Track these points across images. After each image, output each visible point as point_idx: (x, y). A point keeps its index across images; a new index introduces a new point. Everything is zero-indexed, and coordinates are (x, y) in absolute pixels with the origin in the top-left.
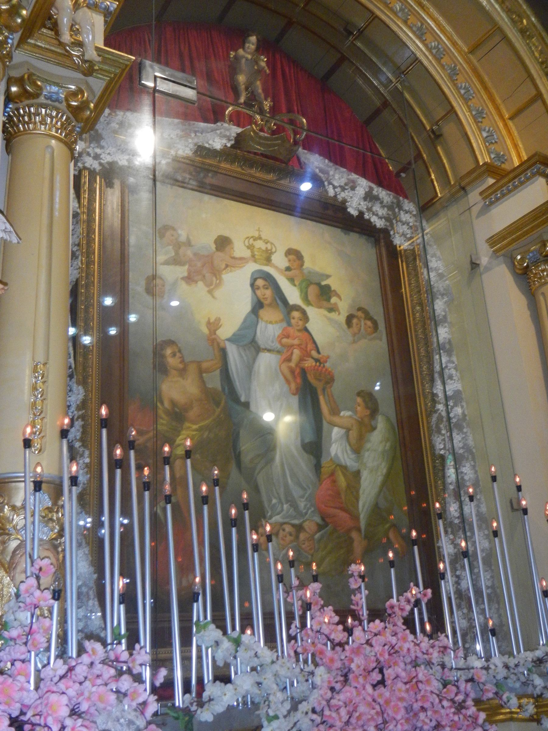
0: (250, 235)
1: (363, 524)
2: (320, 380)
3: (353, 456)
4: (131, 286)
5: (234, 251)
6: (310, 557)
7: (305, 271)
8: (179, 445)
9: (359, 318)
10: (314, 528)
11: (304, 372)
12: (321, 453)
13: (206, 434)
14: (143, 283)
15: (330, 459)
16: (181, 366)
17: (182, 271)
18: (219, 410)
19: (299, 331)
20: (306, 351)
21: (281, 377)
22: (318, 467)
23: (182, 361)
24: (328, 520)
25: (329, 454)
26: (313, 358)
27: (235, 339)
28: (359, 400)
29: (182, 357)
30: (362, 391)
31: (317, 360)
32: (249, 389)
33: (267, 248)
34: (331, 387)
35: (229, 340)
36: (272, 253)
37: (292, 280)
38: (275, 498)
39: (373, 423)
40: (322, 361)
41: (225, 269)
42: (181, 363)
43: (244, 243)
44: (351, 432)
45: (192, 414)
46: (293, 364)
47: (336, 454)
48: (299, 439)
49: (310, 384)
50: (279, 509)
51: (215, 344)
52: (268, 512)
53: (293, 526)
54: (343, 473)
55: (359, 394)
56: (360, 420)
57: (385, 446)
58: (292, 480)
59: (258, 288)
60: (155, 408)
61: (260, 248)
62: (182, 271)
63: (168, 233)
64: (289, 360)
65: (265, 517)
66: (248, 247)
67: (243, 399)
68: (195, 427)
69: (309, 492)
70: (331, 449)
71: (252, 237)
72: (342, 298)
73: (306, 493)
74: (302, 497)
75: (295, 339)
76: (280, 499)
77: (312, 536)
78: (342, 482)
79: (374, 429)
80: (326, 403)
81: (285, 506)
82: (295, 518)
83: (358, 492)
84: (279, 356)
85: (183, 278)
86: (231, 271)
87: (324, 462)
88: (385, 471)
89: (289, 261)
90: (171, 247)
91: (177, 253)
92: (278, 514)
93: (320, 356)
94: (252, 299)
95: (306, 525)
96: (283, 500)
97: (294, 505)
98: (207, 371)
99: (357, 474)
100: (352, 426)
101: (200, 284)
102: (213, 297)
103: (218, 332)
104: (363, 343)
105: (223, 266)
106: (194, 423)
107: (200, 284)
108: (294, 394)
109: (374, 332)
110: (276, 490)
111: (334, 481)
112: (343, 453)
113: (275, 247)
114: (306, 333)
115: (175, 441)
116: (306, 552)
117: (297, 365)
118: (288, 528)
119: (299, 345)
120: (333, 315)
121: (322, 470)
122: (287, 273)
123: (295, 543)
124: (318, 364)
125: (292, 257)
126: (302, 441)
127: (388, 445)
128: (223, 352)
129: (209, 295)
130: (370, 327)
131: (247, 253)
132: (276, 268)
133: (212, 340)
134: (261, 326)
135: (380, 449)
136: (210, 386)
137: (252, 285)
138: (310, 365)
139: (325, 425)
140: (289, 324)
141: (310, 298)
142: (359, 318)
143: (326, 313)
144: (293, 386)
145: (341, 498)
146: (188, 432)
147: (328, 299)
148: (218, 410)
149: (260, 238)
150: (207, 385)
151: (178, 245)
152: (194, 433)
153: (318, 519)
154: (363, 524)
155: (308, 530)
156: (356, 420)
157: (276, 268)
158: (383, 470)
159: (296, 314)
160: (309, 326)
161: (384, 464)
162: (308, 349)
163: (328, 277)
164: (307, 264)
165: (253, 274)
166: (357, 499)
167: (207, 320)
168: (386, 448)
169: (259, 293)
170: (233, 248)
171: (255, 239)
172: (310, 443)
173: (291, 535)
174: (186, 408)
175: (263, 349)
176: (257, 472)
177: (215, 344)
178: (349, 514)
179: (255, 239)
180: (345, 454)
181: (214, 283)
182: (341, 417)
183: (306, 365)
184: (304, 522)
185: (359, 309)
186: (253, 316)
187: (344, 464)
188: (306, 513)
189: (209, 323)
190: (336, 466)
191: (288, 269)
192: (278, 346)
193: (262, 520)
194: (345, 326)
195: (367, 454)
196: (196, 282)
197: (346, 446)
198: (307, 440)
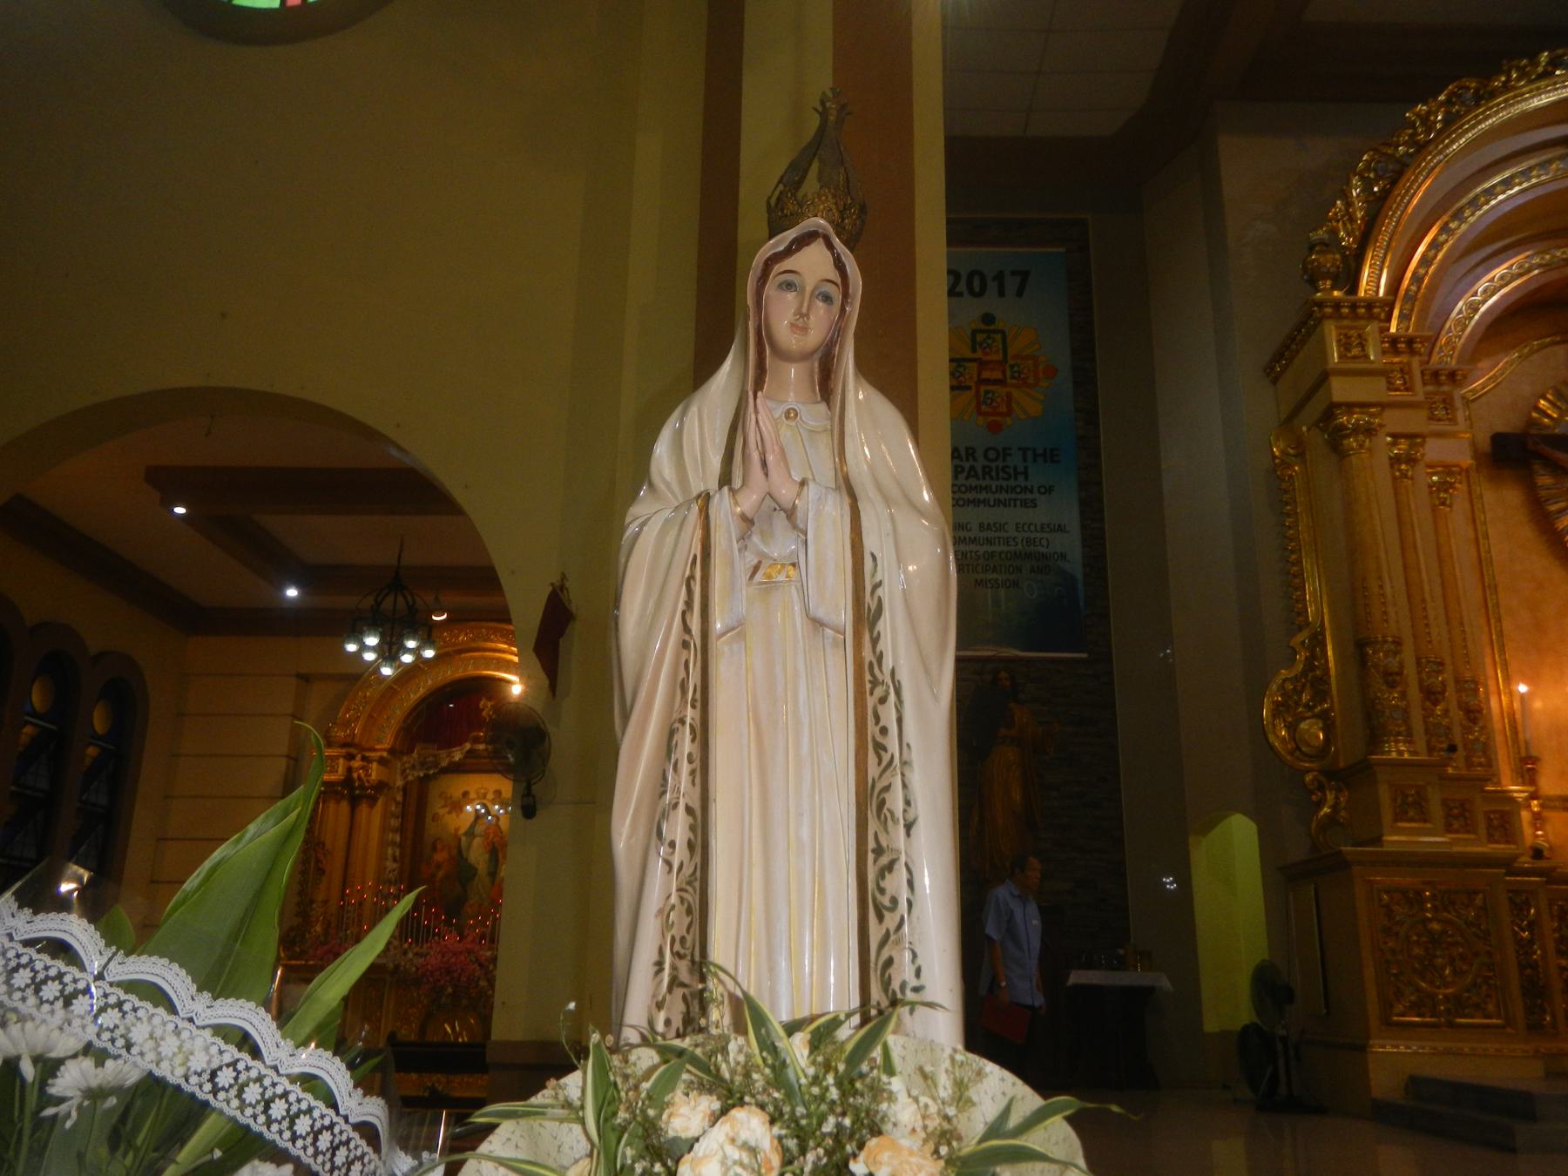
11: (493, 843)
17: (447, 809)
22: (493, 882)
27: (465, 834)
64: (488, 838)
67: (465, 856)
128: (460, 839)
131: (475, 796)
160: (500, 823)
191: (493, 799)
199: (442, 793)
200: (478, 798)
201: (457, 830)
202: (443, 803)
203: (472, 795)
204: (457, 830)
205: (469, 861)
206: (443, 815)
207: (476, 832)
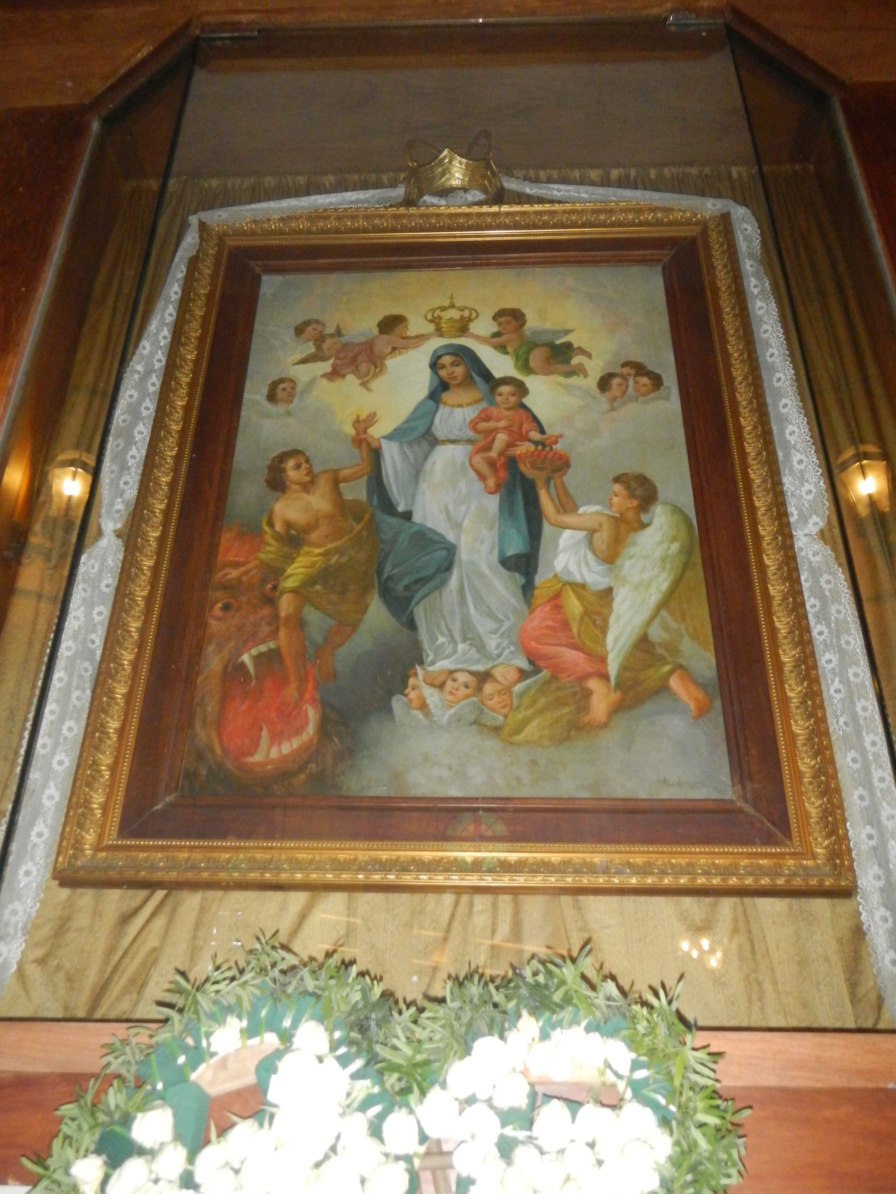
0: (435, 306)
1: (613, 667)
2: (542, 469)
3: (600, 568)
4: (246, 396)
5: (408, 329)
6: (501, 718)
7: (527, 333)
8: (290, 576)
9: (623, 377)
10: (513, 675)
11: (512, 463)
12: (536, 568)
13: (334, 560)
14: (265, 391)
15: (552, 575)
16: (307, 479)
17: (326, 367)
18: (360, 526)
19: (508, 409)
20: (520, 433)
21: (472, 474)
22: (528, 589)
23: (310, 472)
24: (542, 664)
25: (553, 568)
26: (530, 441)
28: (617, 487)
29: (311, 467)
30: (625, 475)
31: (536, 443)
32: (414, 496)
33: (462, 316)
34: (562, 476)
35: (385, 437)
36: (470, 320)
37: (502, 348)
38: (442, 634)
39: (644, 518)
40: (547, 443)
41: (391, 353)
42: (307, 474)
43: (426, 317)
44: (597, 536)
45: (314, 536)
46: (494, 454)
47: (566, 569)
48: (496, 552)
49: (523, 476)
50: (449, 649)
51: (364, 446)
52: (428, 656)
53: (472, 673)
54: (574, 591)
55: (617, 480)
56: (617, 515)
57: (669, 548)
58: (476, 607)
59: (443, 367)
60: (261, 533)
61: (451, 319)
62: (326, 367)
63: (309, 330)
64: (488, 448)
65: (421, 663)
66: (431, 321)
67: (401, 509)
68: (317, 551)
69: (507, 624)
70: (556, 563)
71: (439, 308)
72: (593, 354)
73: (502, 626)
74: (494, 632)
75: (501, 420)
76: (452, 636)
77: (508, 690)
78: (574, 606)
79: (643, 526)
80: (552, 500)
81: (461, 647)
82: (477, 662)
83: (606, 621)
84: (470, 447)
85: (323, 376)
86: (400, 354)
87: (539, 579)
88: (665, 586)
89: (500, 324)
90: (311, 344)
91: (319, 347)
92: (447, 658)
93: (545, 436)
94: (431, 380)
95: (497, 673)
96: (458, 637)
97: (479, 646)
98: (346, 480)
99: (607, 594)
100: (600, 525)
101: (351, 379)
102: (368, 389)
103: (370, 431)
104: (632, 409)
105: (389, 349)
106: (319, 546)
107: (351, 379)
108: (491, 493)
109: (654, 391)
110: (446, 625)
111: (558, 608)
112: (579, 565)
113: (476, 311)
114: (521, 411)
115: (285, 571)
116: (494, 710)
117: (501, 454)
118: (462, 678)
119: (505, 428)
120: (575, 380)
121: (536, 592)
122: (494, 340)
123: (475, 699)
124: (540, 447)
125: (503, 320)
126: (501, 553)
127: (675, 547)
128: (376, 455)
129: (362, 388)
130: (645, 385)
131: (431, 328)
132: (476, 337)
133: (361, 440)
134: (443, 411)
135: (658, 553)
136: (348, 496)
137: (434, 365)
138: (524, 451)
139: (547, 528)
140: (492, 403)
141: (532, 364)
142: (624, 377)
143: (561, 379)
144: (491, 482)
145: (571, 630)
146: (307, 558)
147: (567, 361)
148: (358, 527)
149: (452, 306)
150: (345, 497)
151: (320, 340)
152: (316, 559)
153: (523, 664)
154: (613, 667)
155: (500, 679)
156: (608, 515)
157: (476, 337)
158: (663, 582)
159: (505, 389)
160: (527, 401)
161: (664, 575)
162: (524, 431)
163: (567, 332)
164: (532, 323)
165: (435, 352)
166: (604, 631)
167: (355, 417)
168: (670, 552)
169: (443, 373)
170: (406, 327)
171: (443, 309)
172: (518, 556)
173: (467, 687)
174: (308, 529)
175: (443, 441)
176: (414, 601)
177: (364, 446)
178: (584, 653)
179: (443, 309)
180: (583, 565)
181: (372, 373)
182: (580, 515)
183: (518, 452)
184: (493, 667)
185: (624, 365)
186: (431, 403)
187: (579, 579)
188: (499, 656)
189: (357, 421)
190: (564, 585)
191: (495, 335)
192: (471, 434)
193: (417, 667)
194: (597, 391)
195: (628, 564)
196: (343, 376)
197: (585, 556)
198: (510, 552)
199: (307, 323)
200: (439, 332)
201: (363, 424)
202: (311, 348)
203: (417, 325)
204: (363, 424)
205: (417, 518)
206: (312, 382)
207: (440, 428)
